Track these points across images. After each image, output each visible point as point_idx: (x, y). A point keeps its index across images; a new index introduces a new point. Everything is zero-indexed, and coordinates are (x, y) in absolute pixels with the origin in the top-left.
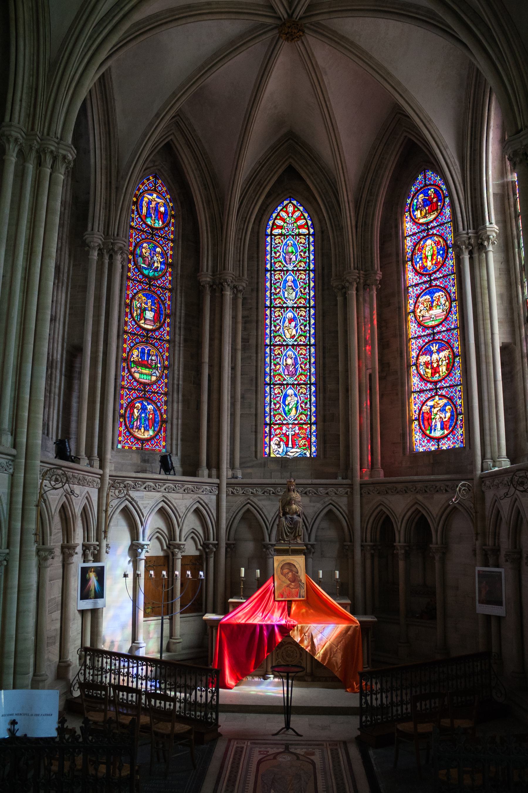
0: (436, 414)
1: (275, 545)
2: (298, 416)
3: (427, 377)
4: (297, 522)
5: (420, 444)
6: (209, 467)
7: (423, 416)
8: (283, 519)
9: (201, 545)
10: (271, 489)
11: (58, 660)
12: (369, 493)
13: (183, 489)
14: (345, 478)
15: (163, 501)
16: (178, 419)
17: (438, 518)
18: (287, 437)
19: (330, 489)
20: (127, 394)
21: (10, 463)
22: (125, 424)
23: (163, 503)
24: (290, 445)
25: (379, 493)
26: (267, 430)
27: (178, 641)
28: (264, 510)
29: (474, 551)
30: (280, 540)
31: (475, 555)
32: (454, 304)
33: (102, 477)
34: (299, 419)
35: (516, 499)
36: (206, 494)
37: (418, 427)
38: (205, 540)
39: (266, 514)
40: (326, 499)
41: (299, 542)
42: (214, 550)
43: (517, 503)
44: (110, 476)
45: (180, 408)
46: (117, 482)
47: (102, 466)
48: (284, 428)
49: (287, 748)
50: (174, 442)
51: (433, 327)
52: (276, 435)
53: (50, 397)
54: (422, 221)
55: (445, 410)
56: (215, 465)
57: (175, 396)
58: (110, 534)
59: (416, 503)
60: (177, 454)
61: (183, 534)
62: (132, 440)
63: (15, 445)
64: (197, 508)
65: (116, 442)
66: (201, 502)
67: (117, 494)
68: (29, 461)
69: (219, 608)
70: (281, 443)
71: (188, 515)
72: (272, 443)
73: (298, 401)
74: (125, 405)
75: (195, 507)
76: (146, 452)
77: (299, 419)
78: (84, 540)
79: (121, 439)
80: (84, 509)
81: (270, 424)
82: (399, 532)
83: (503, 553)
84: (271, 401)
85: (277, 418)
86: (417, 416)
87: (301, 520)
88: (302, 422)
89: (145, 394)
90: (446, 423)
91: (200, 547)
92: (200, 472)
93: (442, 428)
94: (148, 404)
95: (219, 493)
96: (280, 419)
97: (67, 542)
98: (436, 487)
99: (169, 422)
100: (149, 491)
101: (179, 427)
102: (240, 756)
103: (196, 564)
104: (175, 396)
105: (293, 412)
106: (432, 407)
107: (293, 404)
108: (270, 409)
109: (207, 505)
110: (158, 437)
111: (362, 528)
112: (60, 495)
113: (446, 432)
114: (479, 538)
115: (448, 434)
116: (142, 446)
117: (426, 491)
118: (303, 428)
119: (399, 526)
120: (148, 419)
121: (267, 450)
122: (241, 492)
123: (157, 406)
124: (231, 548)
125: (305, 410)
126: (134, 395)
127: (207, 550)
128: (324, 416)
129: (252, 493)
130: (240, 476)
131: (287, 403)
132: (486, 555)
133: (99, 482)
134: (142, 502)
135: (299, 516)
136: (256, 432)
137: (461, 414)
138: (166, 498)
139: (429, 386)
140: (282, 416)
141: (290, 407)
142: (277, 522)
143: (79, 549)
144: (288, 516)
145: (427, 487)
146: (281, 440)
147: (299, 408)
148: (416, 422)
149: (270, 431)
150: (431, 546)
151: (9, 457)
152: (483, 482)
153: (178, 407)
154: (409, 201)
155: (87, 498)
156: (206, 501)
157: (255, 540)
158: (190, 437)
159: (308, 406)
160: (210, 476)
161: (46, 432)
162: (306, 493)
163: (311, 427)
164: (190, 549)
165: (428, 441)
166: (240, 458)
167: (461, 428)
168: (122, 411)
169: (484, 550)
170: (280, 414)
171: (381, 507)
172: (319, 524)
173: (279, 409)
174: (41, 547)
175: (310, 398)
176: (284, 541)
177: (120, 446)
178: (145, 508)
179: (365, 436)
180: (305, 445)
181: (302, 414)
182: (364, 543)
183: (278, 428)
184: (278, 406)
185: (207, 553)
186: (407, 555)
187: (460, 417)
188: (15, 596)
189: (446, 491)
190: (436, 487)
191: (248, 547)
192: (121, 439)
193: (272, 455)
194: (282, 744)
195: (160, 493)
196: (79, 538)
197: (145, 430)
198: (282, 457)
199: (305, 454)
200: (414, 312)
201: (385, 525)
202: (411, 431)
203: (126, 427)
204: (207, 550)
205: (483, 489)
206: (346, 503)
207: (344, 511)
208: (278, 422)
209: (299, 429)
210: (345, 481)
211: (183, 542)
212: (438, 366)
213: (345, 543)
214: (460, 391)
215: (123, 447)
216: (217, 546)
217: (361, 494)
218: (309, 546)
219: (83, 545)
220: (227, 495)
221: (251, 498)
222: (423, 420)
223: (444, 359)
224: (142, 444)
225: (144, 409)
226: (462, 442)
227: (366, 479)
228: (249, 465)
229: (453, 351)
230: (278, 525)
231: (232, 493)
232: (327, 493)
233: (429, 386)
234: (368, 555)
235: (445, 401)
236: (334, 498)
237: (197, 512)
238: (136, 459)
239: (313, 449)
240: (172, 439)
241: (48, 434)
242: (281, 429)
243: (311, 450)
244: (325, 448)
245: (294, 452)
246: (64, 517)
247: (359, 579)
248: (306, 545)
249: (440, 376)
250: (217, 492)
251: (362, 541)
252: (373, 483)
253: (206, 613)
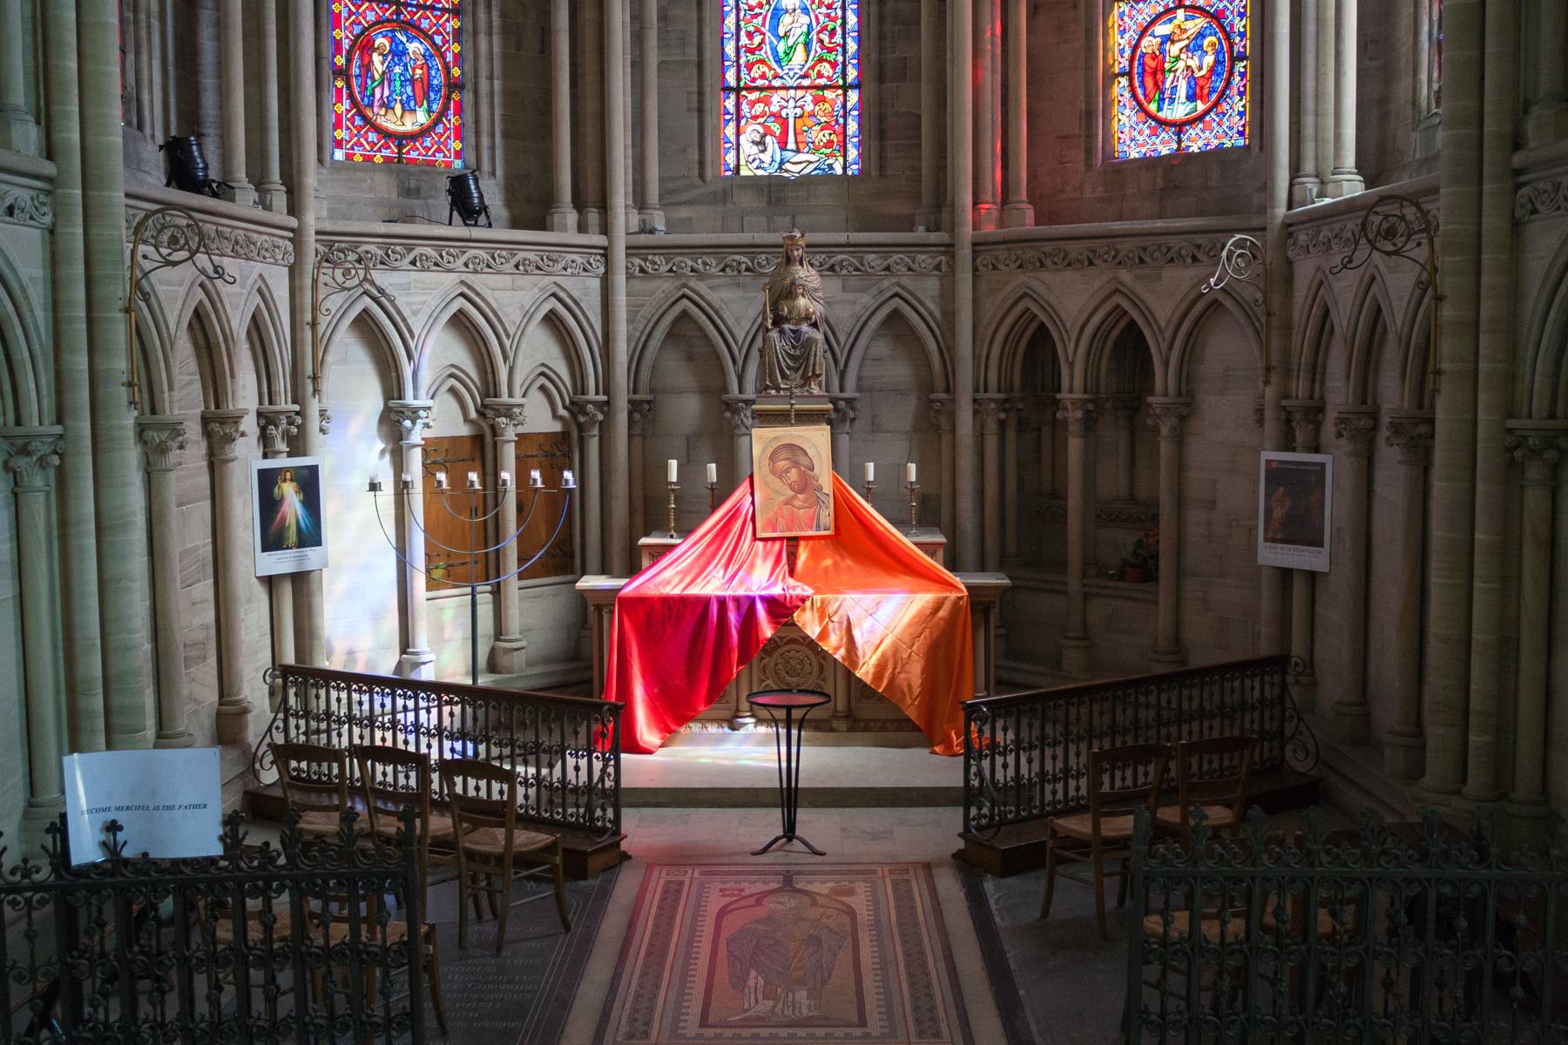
0: (1178, 58)
1: (753, 402)
2: (812, 68)
4: (810, 342)
5: (1132, 136)
6: (579, 204)
7: (1143, 65)
8: (774, 334)
9: (565, 407)
10: (744, 259)
11: (215, 698)
12: (995, 268)
13: (513, 262)
14: (935, 227)
15: (462, 295)
16: (491, 78)
17: (1171, 328)
18: (784, 123)
19: (895, 257)
20: (351, 13)
21: (42, 198)
22: (351, 96)
23: (461, 299)
24: (791, 145)
25: (1020, 266)
26: (730, 104)
27: (515, 645)
28: (726, 314)
29: (1260, 412)
30: (767, 387)
31: (1260, 421)
33: (297, 237)
34: (813, 74)
35: (1373, 279)
36: (573, 275)
37: (1127, 95)
38: (575, 393)
39: (730, 322)
40: (886, 283)
41: (816, 390)
42: (600, 417)
43: (1374, 289)
44: (318, 233)
45: (496, 50)
46: (336, 247)
47: (294, 209)
48: (776, 98)
49: (788, 880)
50: (485, 141)
52: (755, 118)
53: (136, 22)
55: (1201, 47)
56: (593, 198)
57: (482, 15)
58: (327, 385)
59: (1117, 291)
60: (493, 173)
61: (518, 380)
62: (372, 137)
63: (50, 153)
64: (552, 311)
65: (328, 143)
66: (562, 295)
67: (340, 279)
68: (93, 193)
69: (617, 559)
70: (768, 139)
71: (529, 330)
72: (742, 138)
73: (810, 26)
74: (346, 44)
75: (546, 308)
76: (412, 168)
77: (813, 74)
78: (261, 403)
79: (340, 134)
80: (255, 319)
81: (738, 90)
82: (1071, 365)
83: (1331, 415)
84: (738, 28)
85: (756, 72)
86: (1125, 63)
87: (819, 336)
88: (823, 81)
89: (398, 13)
90: (1201, 82)
91: (562, 412)
92: (556, 218)
93: (1191, 98)
94: (410, 40)
95: (606, 272)
96: (763, 76)
97: (217, 407)
98: (1169, 249)
99: (469, 86)
100: (424, 269)
101: (497, 100)
102: (677, 901)
103: (553, 455)
104: (482, 15)
105: (799, 56)
106: (1168, 39)
107: (798, 32)
108: (738, 49)
109: (577, 303)
110: (440, 129)
111: (976, 356)
112: (187, 283)
113: (1201, 106)
114: (1274, 379)
115: (1207, 112)
116: (400, 153)
117: (1142, 261)
118: (824, 100)
119: (1070, 352)
120: (412, 81)
121: (730, 158)
122: (664, 268)
123: (434, 44)
124: (644, 411)
125: (830, 50)
126: (371, 16)
127: (582, 419)
128: (881, 66)
129: (693, 270)
130: (660, 225)
131: (781, 32)
132: (1288, 421)
133: (290, 248)
134: (407, 299)
135: (815, 325)
136: (701, 110)
137: (1242, 57)
138: (469, 287)
140: (771, 68)
141: (791, 42)
142: (759, 342)
143: (250, 424)
144: (786, 326)
145: (1144, 249)
146: (768, 132)
147: (815, 46)
148: (1124, 81)
149: (738, 105)
150: (1150, 399)
151: (39, 184)
152: (1290, 235)
153: (490, 46)
155: (259, 291)
156: (575, 293)
157: (703, 391)
158: (528, 124)
159: (838, 39)
160: (582, 228)
161: (135, 120)
162: (832, 268)
163: (845, 95)
164: (539, 418)
165: (1154, 134)
166: (661, 180)
167: (1241, 94)
168: (340, 61)
169: (1284, 408)
170: (762, 61)
171: (1026, 303)
172: (868, 347)
173: (759, 47)
174: (148, 418)
175: (844, 17)
176: (778, 389)
177: (339, 155)
178: (415, 313)
179: (988, 116)
180: (829, 144)
181: (821, 60)
182: (981, 395)
183: (759, 101)
184: (757, 39)
185: (581, 428)
186: (1089, 423)
187: (1240, 67)
188: (91, 542)
189: (1195, 259)
190: (1169, 249)
191: (686, 409)
192: (340, 134)
193: (744, 172)
194: (777, 873)
195: (453, 278)
196: (245, 394)
197: (404, 110)
198: (770, 176)
199: (831, 167)
201: (1036, 347)
202: (1108, 105)
203: (354, 103)
204: (582, 419)
205: (1289, 254)
206: (936, 293)
207: (931, 314)
208: (759, 82)
209: (816, 101)
210: (933, 237)
211: (517, 400)
213: (933, 396)
215: (349, 157)
216: (607, 406)
217: (975, 269)
218: (842, 404)
219: (259, 414)
220: (630, 277)
221: (691, 284)
222: (1142, 75)
224: (400, 147)
225: (398, 53)
226: (1241, 133)
227: (990, 229)
228: (684, 197)
230: (761, 351)
231: (642, 270)
232: (887, 268)
234: (991, 426)
235: (1201, 22)
236: (905, 281)
237: (552, 320)
238: (384, 187)
239: (853, 153)
240: (477, 133)
241: (140, 127)
242: (767, 102)
243: (845, 156)
244: (882, 149)
245: (800, 164)
246: (201, 341)
247: (966, 484)
248: (834, 401)
250: (602, 270)
251: (976, 390)
252: (1005, 242)
253: (583, 573)
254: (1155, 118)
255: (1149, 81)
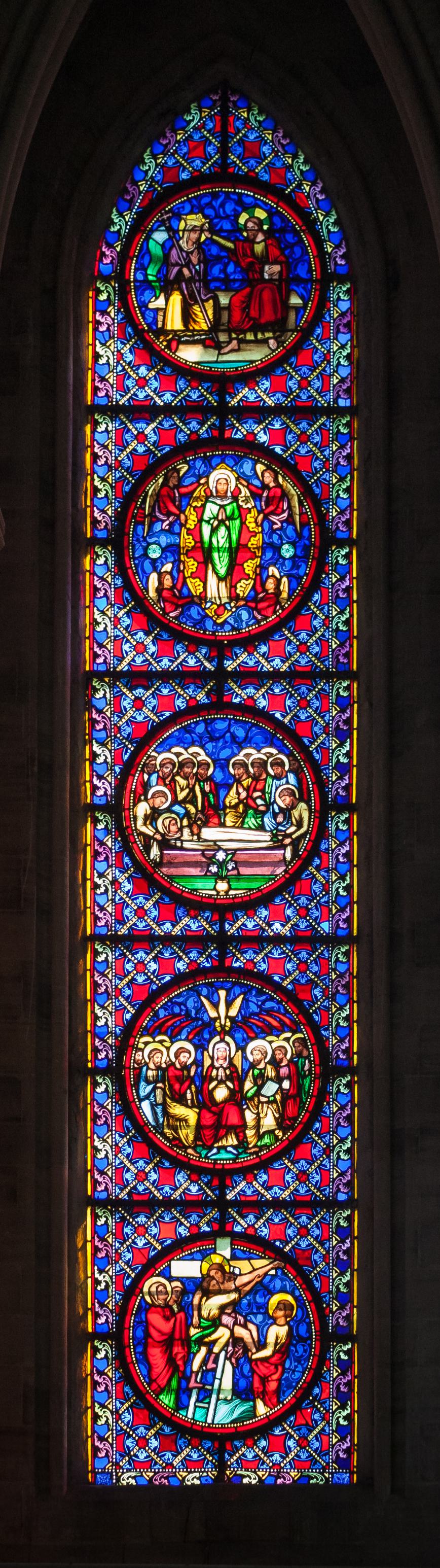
0: (216, 1323)
3: (177, 1142)
32: (338, 822)
51: (223, 909)
54: (191, 354)
90: (263, 1370)
93: (242, 1392)
106: (192, 1286)
137: (343, 1336)
139: (185, 1185)
148: (104, 1350)
154: (120, 223)
187: (341, 1351)
200: (116, 809)
212: (238, 1099)
214: (344, 1233)
223: (270, 1072)
229: (321, 1043)
233: (185, 1185)
249: (243, 1143)
254: (168, 1420)
255: (157, 1356)
